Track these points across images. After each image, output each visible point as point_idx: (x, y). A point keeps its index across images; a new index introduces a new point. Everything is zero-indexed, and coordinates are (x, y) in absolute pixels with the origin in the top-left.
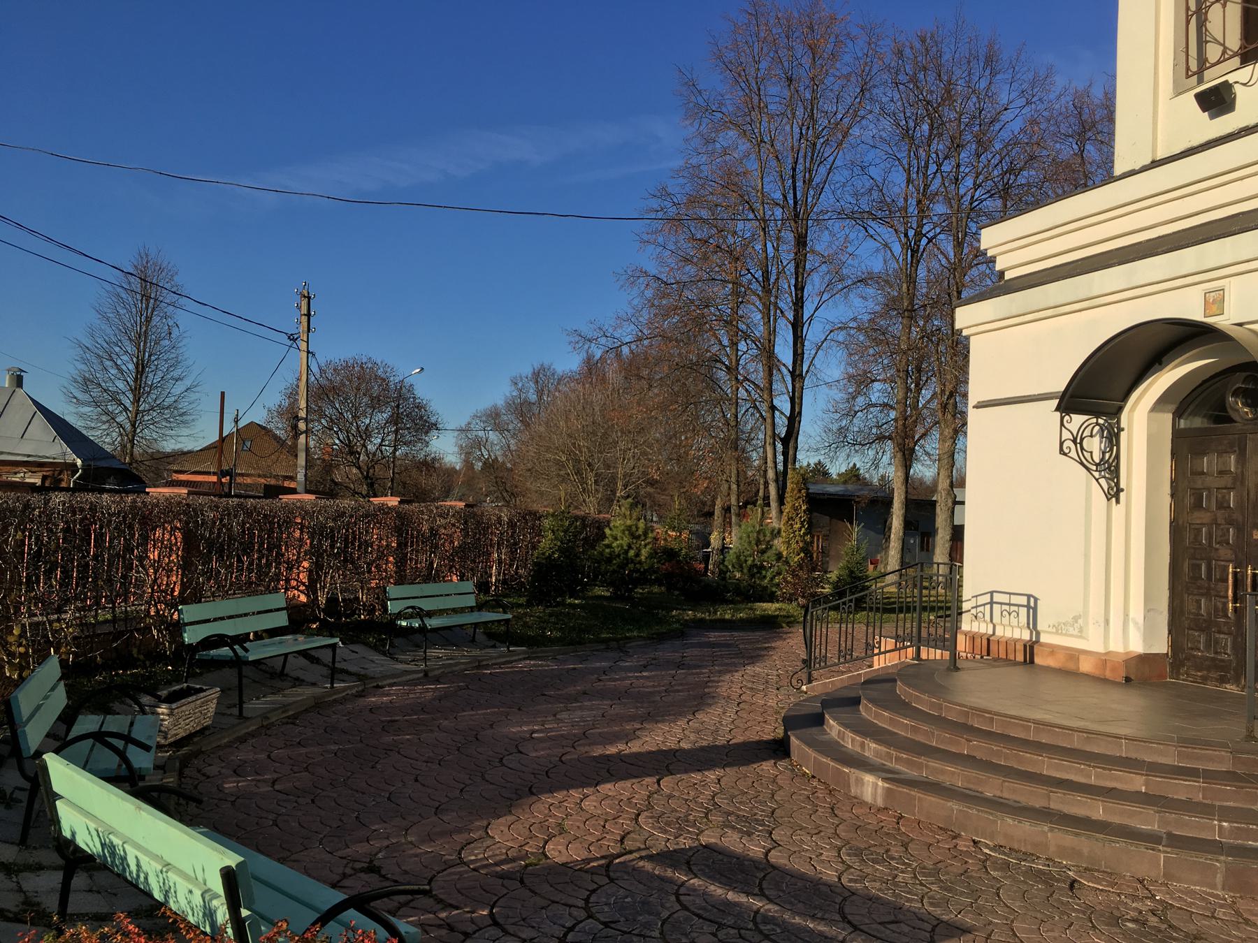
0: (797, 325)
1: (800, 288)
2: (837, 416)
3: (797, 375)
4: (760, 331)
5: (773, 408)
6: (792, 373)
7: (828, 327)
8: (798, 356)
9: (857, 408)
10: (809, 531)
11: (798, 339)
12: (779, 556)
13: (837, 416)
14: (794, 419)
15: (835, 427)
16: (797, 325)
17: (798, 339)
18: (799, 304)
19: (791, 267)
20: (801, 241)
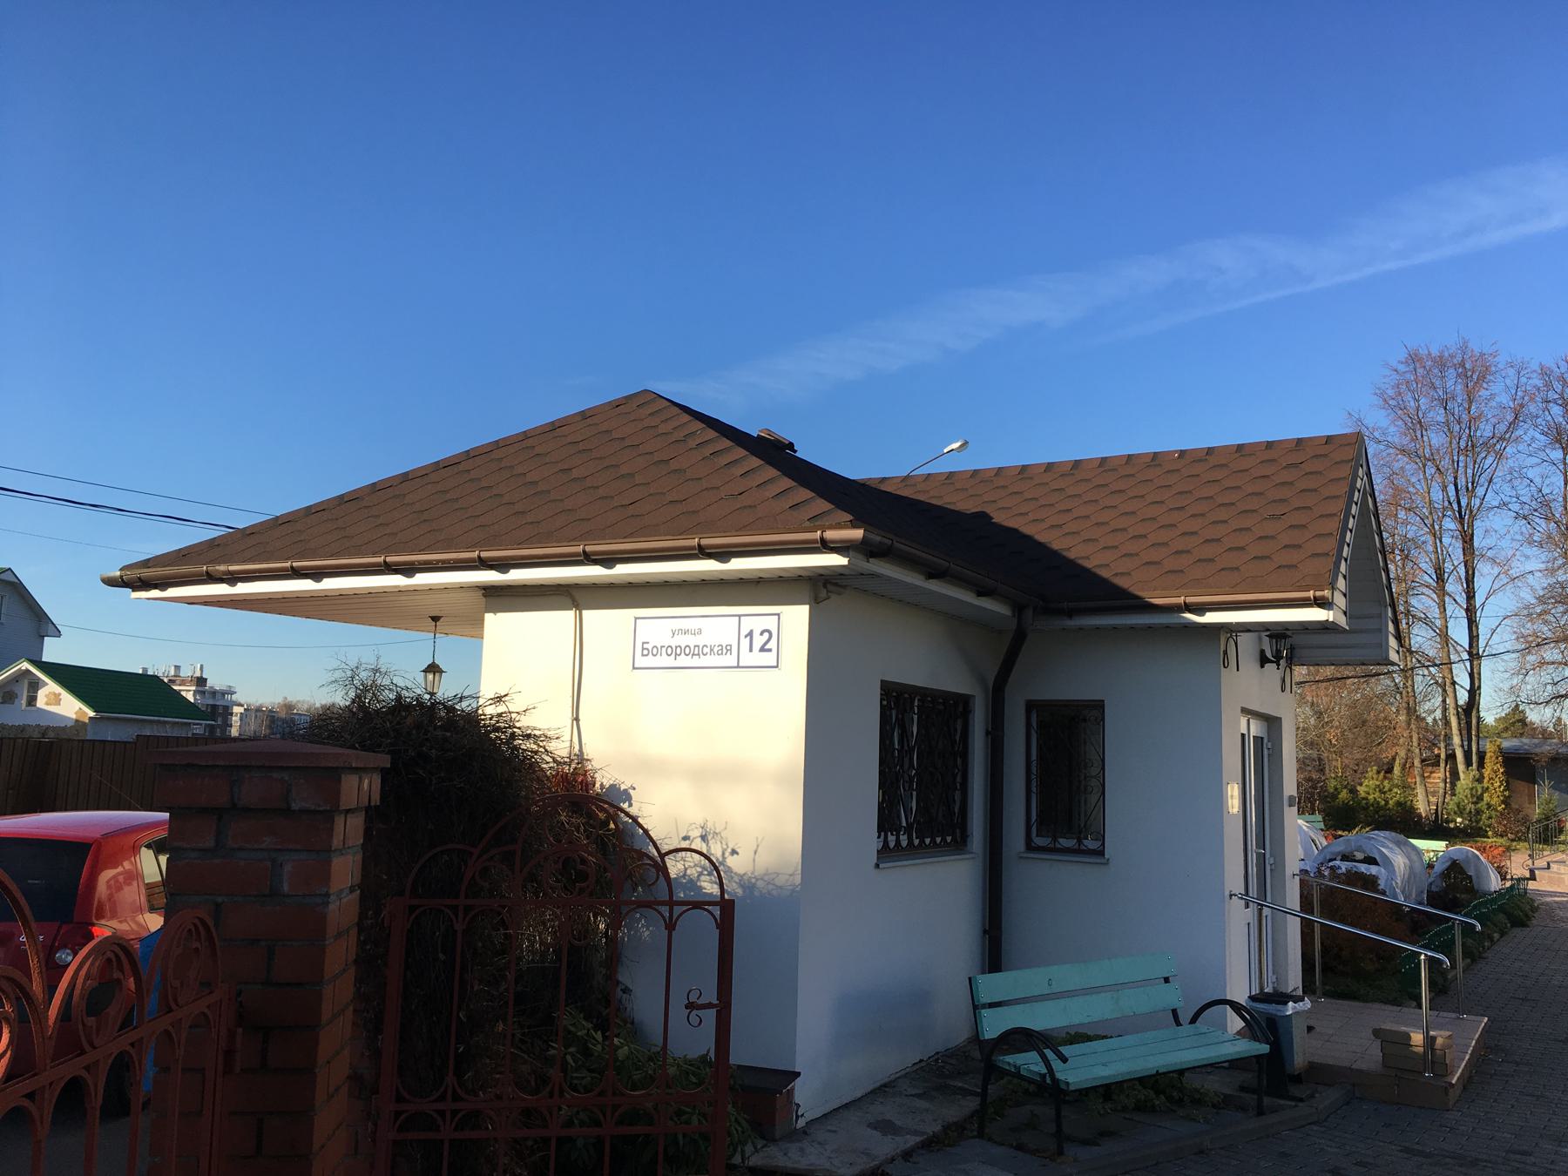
0: (1471, 613)
1: (1470, 580)
2: (1507, 675)
3: (1474, 656)
4: (1434, 612)
5: (1454, 683)
6: (1470, 653)
7: (1502, 613)
8: (1473, 638)
9: (1528, 666)
10: (1507, 788)
11: (1472, 623)
12: (1489, 806)
13: (1507, 675)
14: (1474, 692)
15: (1506, 687)
16: (1471, 613)
17: (1472, 623)
18: (1470, 595)
19: (1462, 568)
20: (1467, 540)
